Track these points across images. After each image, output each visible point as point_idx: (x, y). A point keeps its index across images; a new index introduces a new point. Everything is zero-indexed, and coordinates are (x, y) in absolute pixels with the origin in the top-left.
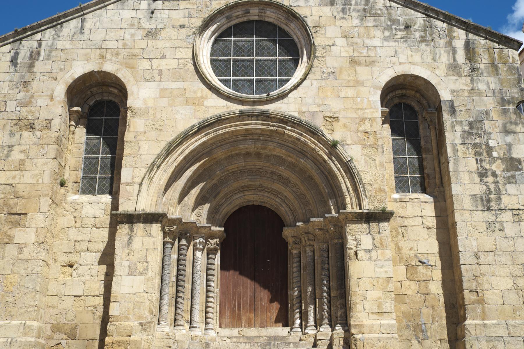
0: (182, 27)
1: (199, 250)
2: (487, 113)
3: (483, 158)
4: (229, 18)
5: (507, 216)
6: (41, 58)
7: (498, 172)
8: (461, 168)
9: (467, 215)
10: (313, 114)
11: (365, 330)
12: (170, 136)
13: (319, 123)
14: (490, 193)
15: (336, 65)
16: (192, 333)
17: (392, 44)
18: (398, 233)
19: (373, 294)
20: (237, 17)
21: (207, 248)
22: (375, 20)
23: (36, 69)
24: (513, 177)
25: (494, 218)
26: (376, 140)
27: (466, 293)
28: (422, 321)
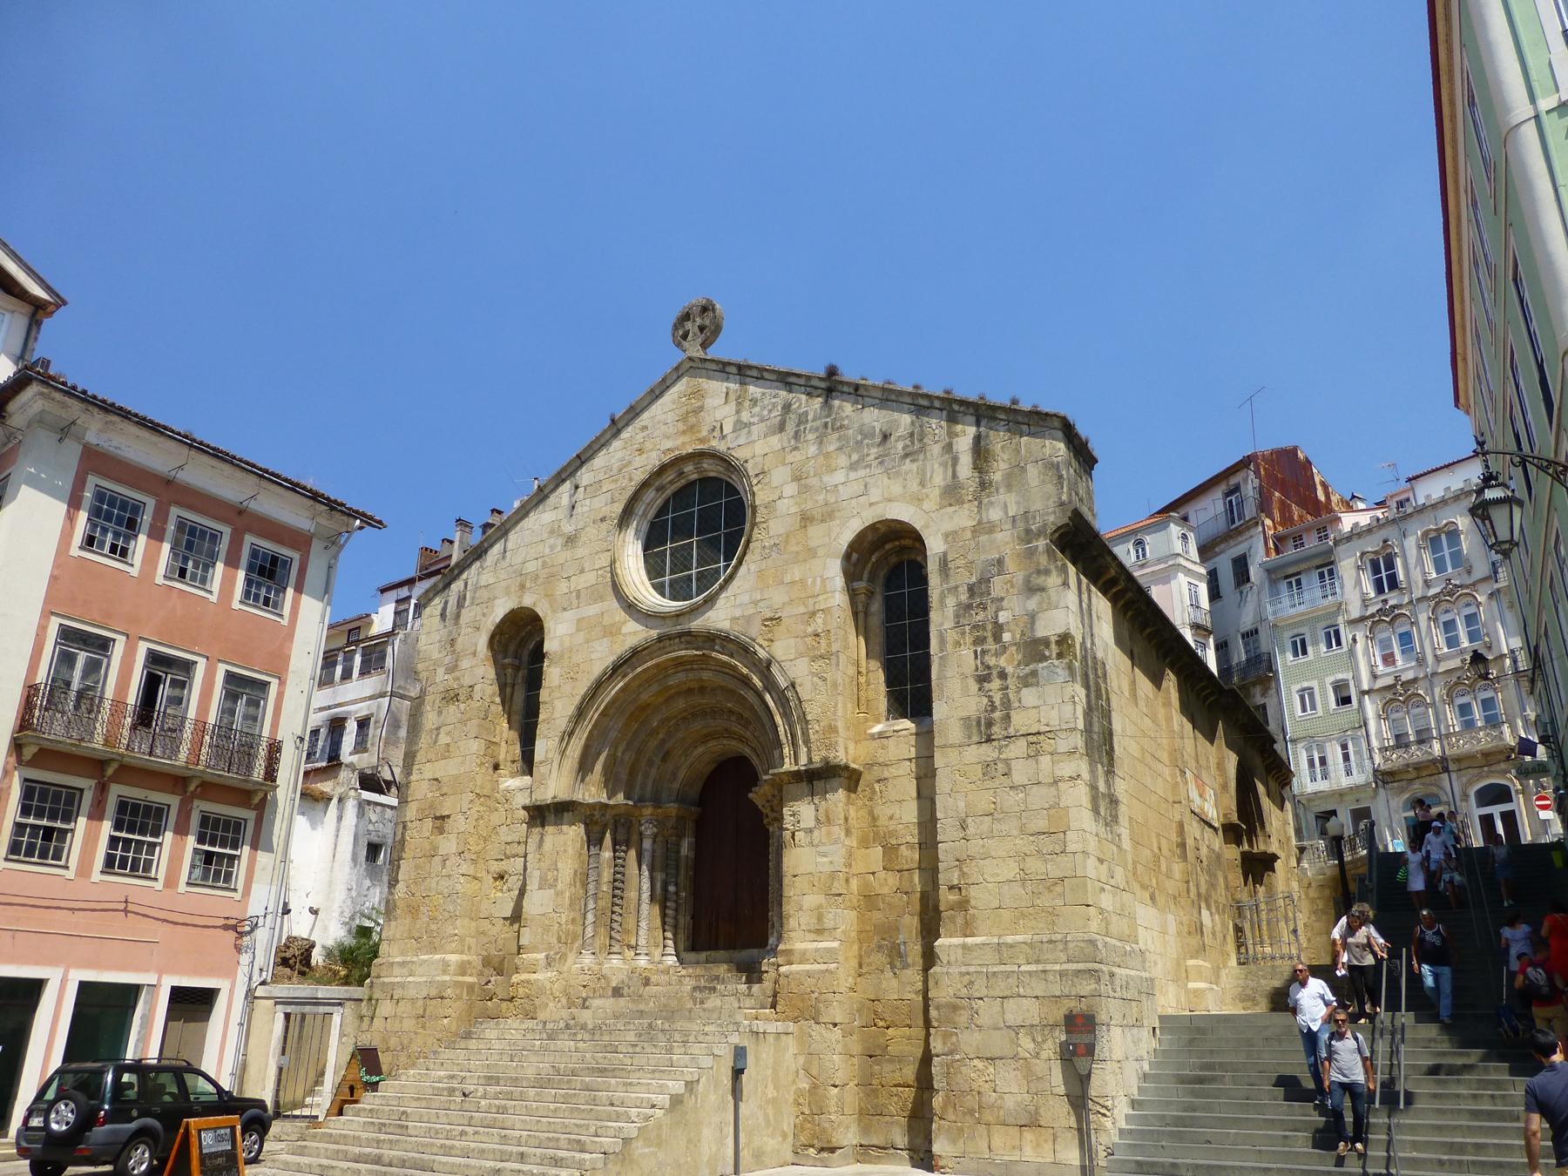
0: (603, 520)
2: (1000, 562)
3: (986, 647)
4: (660, 489)
5: (1018, 748)
6: (467, 603)
7: (1010, 670)
8: (952, 671)
9: (953, 755)
10: (748, 619)
11: (796, 958)
12: (582, 688)
13: (754, 633)
14: (993, 708)
15: (781, 531)
17: (862, 473)
18: (874, 792)
19: (812, 900)
20: (671, 482)
22: (839, 439)
23: (463, 620)
24: (1034, 673)
25: (995, 755)
26: (829, 645)
27: (943, 889)
28: (901, 938)
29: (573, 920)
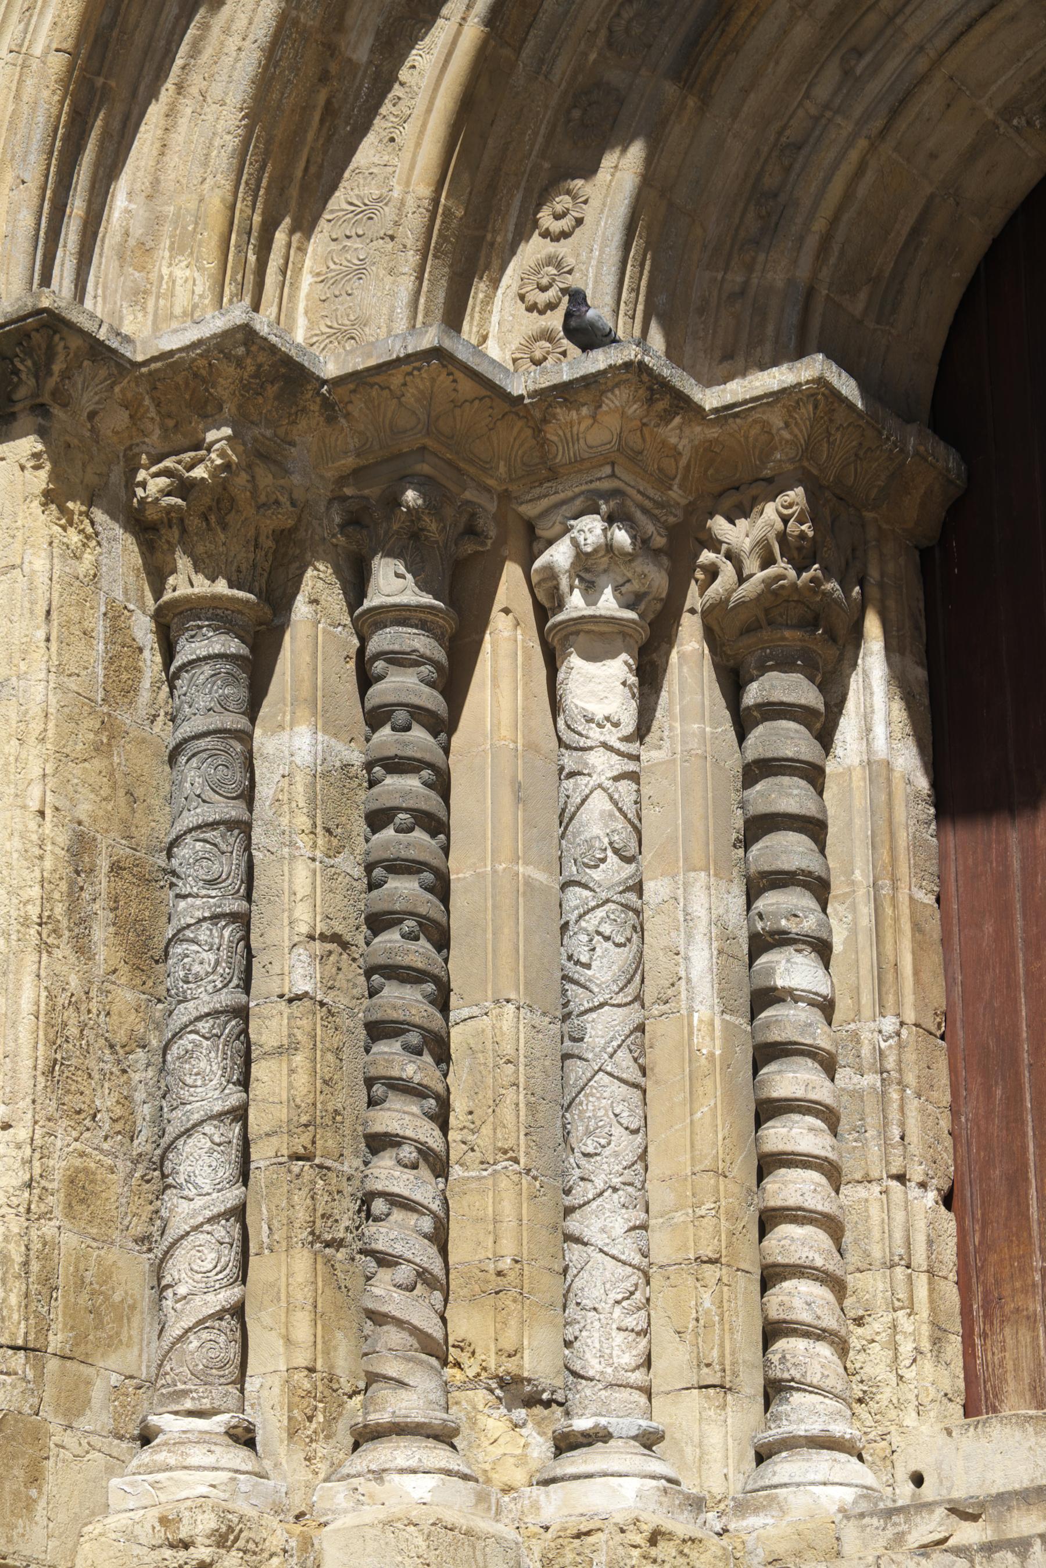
1: (597, 638)
16: (554, 1506)
21: (707, 614)
29: (80, 1190)
